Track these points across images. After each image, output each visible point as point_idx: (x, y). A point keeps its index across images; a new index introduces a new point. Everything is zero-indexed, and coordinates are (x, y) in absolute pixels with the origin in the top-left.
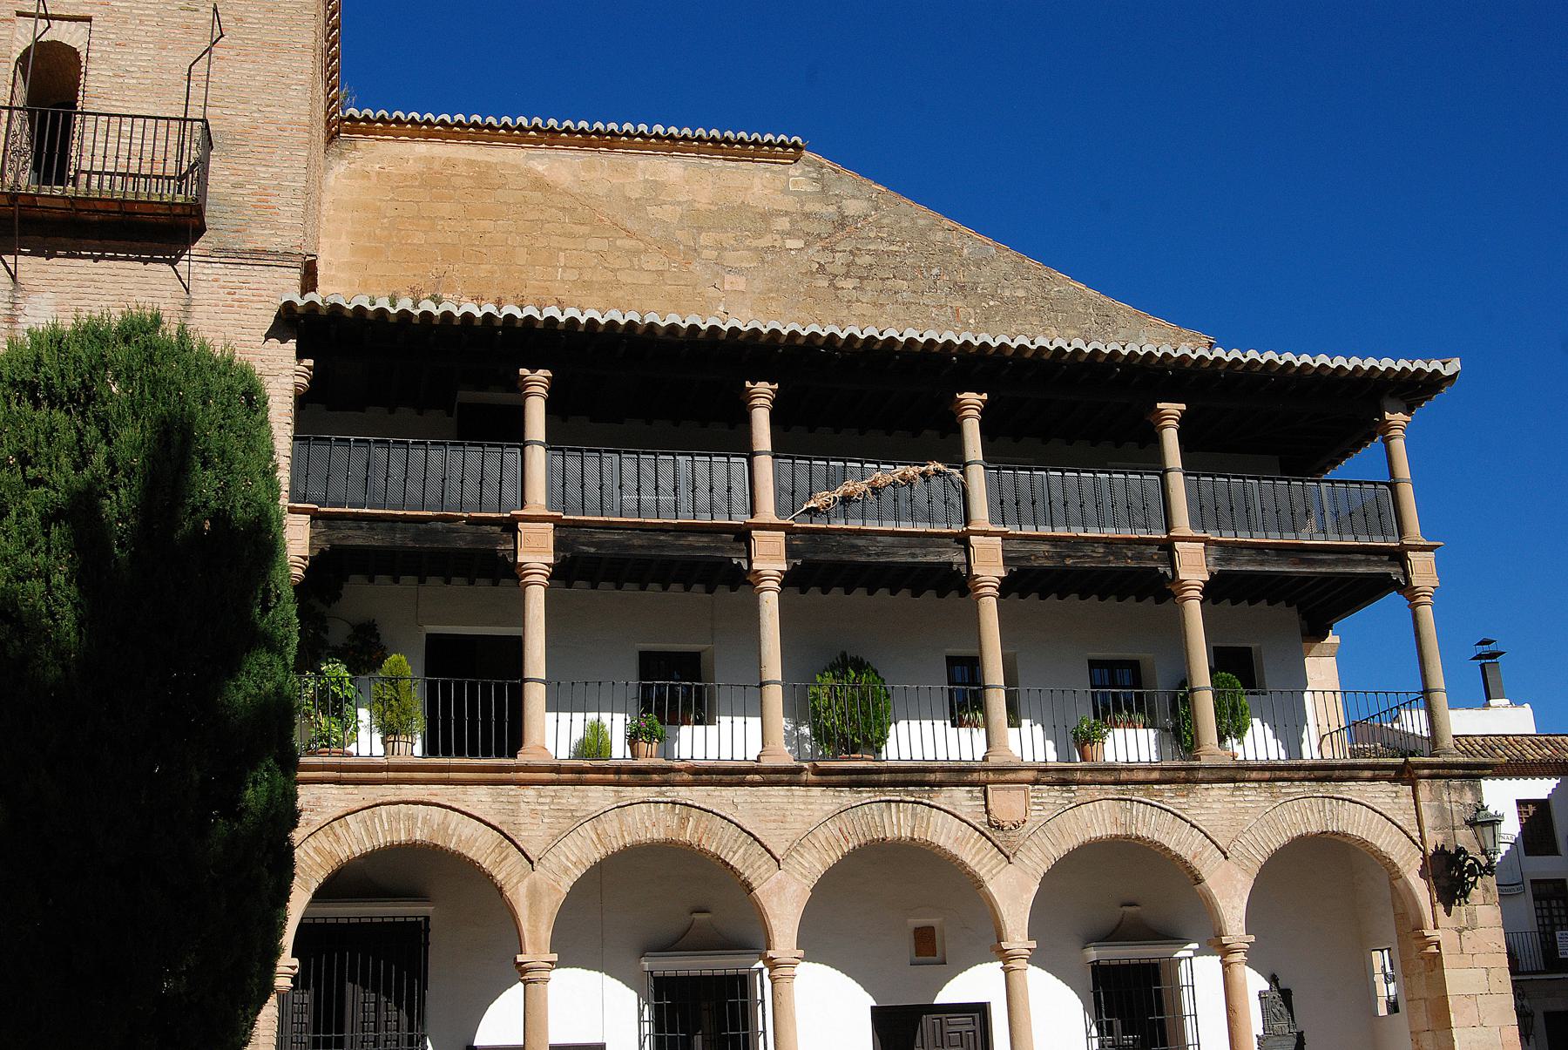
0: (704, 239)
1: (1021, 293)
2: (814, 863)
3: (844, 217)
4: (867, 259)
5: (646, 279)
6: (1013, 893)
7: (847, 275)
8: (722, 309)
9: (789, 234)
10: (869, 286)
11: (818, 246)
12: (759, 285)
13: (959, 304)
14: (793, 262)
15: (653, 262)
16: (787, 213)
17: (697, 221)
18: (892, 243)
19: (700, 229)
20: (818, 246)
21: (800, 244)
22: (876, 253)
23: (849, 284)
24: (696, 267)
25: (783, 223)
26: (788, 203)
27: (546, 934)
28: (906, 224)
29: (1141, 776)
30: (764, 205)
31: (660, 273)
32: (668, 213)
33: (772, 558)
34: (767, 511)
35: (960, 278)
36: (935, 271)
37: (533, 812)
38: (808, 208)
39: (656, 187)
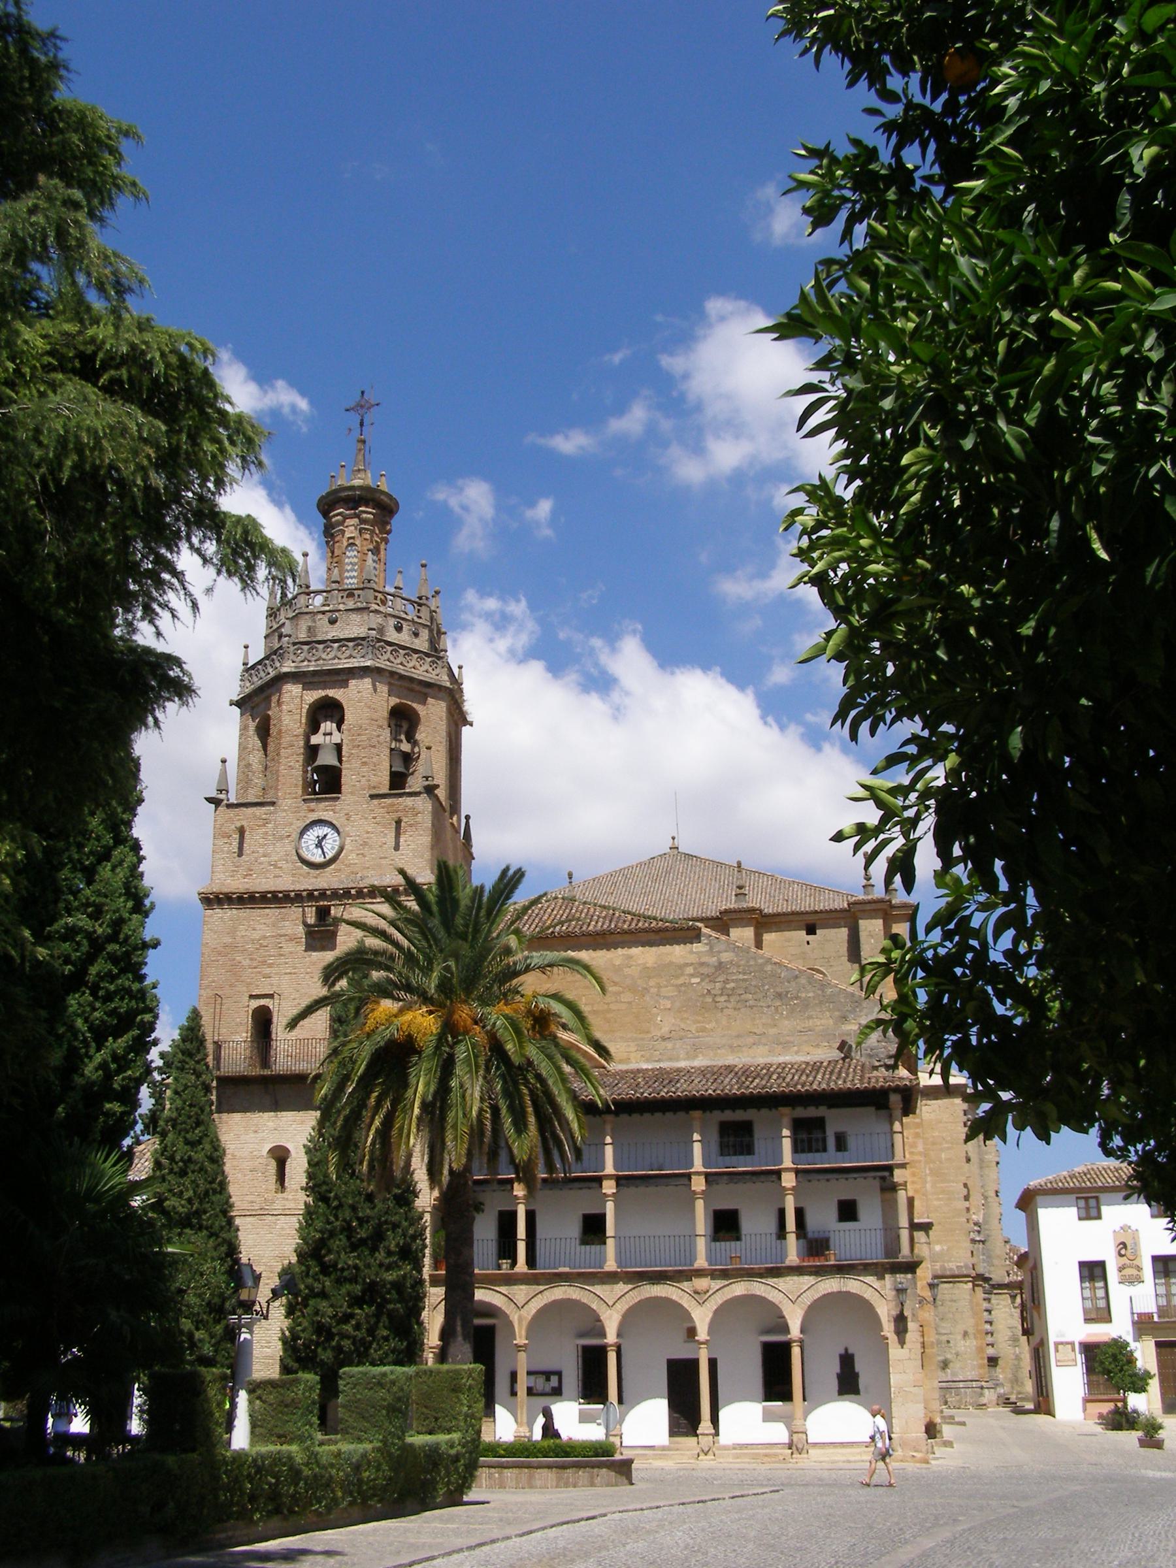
0: (652, 983)
1: (811, 995)
2: (622, 1307)
3: (720, 963)
4: (732, 985)
5: (624, 1006)
6: (702, 1318)
7: (721, 995)
9: (692, 976)
12: (678, 1004)
15: (627, 997)
17: (648, 972)
18: (744, 974)
19: (649, 978)
21: (698, 980)
23: (722, 999)
24: (647, 998)
25: (690, 970)
26: (693, 959)
27: (524, 1333)
28: (752, 963)
30: (682, 961)
31: (630, 1003)
34: (609, 1169)
37: (520, 1292)
38: (703, 960)
39: (630, 957)
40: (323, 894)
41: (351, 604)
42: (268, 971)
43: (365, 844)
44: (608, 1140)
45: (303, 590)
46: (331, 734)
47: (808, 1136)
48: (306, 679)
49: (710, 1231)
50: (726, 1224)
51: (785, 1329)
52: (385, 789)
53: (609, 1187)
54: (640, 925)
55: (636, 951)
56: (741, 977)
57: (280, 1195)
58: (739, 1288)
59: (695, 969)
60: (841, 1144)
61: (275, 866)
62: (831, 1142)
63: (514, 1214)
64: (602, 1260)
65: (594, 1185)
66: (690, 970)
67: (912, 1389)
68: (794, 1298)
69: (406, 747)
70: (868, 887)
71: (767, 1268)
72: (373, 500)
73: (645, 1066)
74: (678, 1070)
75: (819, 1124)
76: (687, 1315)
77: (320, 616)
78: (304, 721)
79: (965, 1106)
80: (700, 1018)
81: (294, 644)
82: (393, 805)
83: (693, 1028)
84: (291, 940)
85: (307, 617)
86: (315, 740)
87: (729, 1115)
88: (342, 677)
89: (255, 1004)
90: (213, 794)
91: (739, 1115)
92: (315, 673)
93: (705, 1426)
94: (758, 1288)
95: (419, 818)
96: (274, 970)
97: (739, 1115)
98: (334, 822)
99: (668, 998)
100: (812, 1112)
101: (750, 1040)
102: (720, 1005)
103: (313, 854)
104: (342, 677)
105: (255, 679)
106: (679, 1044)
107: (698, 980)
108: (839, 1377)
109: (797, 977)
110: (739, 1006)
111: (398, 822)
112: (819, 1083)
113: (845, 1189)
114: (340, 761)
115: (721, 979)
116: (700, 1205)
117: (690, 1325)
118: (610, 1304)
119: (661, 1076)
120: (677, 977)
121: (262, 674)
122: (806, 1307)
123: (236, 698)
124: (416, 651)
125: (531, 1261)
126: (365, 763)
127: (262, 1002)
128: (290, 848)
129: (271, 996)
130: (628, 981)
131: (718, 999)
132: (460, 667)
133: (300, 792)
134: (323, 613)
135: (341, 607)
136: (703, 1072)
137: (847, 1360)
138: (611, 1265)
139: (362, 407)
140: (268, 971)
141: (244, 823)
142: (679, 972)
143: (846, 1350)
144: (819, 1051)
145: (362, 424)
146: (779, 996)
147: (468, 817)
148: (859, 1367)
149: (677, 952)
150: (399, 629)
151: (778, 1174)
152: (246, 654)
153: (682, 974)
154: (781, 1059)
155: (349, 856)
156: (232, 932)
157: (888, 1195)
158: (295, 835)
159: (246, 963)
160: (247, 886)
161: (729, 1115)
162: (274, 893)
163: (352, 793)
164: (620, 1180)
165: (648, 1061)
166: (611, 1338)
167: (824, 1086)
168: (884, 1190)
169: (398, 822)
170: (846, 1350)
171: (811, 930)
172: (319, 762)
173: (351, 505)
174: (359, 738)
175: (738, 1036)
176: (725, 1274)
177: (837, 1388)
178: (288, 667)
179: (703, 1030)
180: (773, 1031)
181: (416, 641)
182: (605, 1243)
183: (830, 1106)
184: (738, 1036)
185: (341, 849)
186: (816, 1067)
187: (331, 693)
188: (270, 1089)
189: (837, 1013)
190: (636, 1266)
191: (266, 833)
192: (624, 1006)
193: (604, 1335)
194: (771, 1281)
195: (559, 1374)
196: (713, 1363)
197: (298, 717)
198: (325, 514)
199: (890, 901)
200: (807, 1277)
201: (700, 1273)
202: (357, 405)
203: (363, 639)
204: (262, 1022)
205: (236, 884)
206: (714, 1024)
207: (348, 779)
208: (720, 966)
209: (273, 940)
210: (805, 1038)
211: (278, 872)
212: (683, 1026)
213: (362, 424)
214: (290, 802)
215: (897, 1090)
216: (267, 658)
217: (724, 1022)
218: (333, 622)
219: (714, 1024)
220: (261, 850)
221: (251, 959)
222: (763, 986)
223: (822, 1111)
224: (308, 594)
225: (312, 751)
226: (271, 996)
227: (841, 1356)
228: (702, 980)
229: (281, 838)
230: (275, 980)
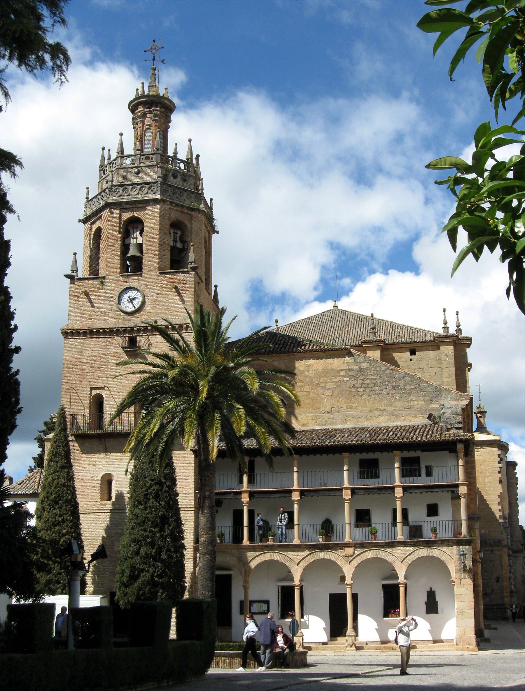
0: (321, 380)
1: (412, 387)
2: (303, 565)
3: (360, 369)
4: (367, 382)
5: (305, 394)
6: (348, 570)
7: (361, 387)
8: (325, 401)
9: (344, 376)
10: (367, 389)
11: (353, 379)
13: (393, 392)
14: (346, 385)
15: (307, 388)
16: (344, 370)
18: (374, 375)
19: (320, 377)
20: (353, 379)
21: (348, 379)
22: (369, 379)
23: (362, 390)
24: (319, 389)
25: (343, 373)
26: (345, 367)
28: (378, 369)
30: (338, 368)
31: (309, 392)
32: (311, 374)
33: (297, 497)
35: (394, 384)
36: (387, 383)
38: (350, 367)
39: (309, 366)
40: (132, 330)
41: (147, 163)
42: (101, 374)
43: (156, 301)
44: (295, 469)
47: (410, 468)
48: (123, 206)
49: (353, 522)
50: (362, 518)
51: (396, 577)
54: (314, 347)
55: (312, 362)
56: (372, 377)
58: (370, 554)
59: (346, 372)
60: (429, 472)
62: (423, 471)
63: (242, 511)
64: (292, 538)
65: (287, 495)
66: (343, 373)
67: (468, 611)
68: (401, 560)
69: (179, 245)
70: (446, 328)
71: (386, 543)
72: (161, 103)
73: (317, 428)
74: (336, 430)
75: (417, 461)
76: (340, 569)
77: (130, 170)
79: (499, 452)
80: (348, 401)
82: (171, 279)
83: (345, 406)
84: (114, 356)
85: (122, 171)
87: (365, 456)
88: (143, 204)
89: (94, 392)
90: (69, 273)
91: (371, 456)
92: (127, 203)
93: (350, 631)
94: (381, 554)
95: (188, 286)
96: (105, 373)
97: (371, 456)
98: (139, 288)
99: (329, 389)
100: (412, 454)
101: (377, 413)
102: (360, 393)
104: (143, 204)
105: (93, 207)
106: (336, 415)
107: (348, 379)
108: (426, 603)
109: (404, 377)
110: (371, 393)
111: (176, 288)
112: (416, 437)
113: (431, 498)
114: (142, 253)
115: (361, 378)
116: (347, 506)
117: (342, 575)
118: (297, 562)
119: (327, 433)
120: (336, 377)
121: (97, 204)
122: (408, 565)
123: (82, 218)
124: (185, 190)
125: (251, 538)
127: (98, 392)
129: (103, 388)
130: (307, 380)
131: (359, 390)
132: (211, 200)
133: (119, 271)
134: (132, 168)
135: (142, 165)
136: (351, 431)
137: (431, 594)
138: (296, 541)
140: (101, 374)
141: (87, 289)
142: (337, 374)
143: (431, 588)
144: (417, 419)
145: (154, 59)
146: (394, 388)
147: (216, 286)
149: (336, 363)
150: (175, 177)
151: (393, 488)
152: (88, 193)
153: (339, 376)
154: (395, 424)
155: (148, 307)
156: (81, 352)
157: (456, 502)
158: (116, 297)
160: (89, 325)
161: (365, 456)
162: (104, 330)
163: (149, 272)
164: (303, 493)
165: (319, 425)
166: (297, 582)
167: (419, 439)
168: (452, 498)
169: (176, 288)
170: (431, 588)
171: (413, 353)
173: (147, 106)
174: (153, 240)
175: (370, 411)
176: (362, 546)
179: (351, 407)
180: (390, 408)
181: (186, 184)
182: (294, 528)
183: (423, 451)
184: (370, 411)
186: (415, 428)
187: (136, 214)
188: (101, 439)
189: (427, 398)
190: (311, 541)
191: (99, 295)
192: (305, 394)
193: (293, 580)
194: (388, 550)
195: (267, 602)
196: (355, 597)
198: (133, 111)
199: (457, 336)
200: (409, 548)
201: (348, 545)
202: (151, 48)
204: (98, 403)
205: (83, 324)
206: (356, 404)
208: (360, 371)
209: (104, 356)
210: (409, 412)
211: (106, 317)
212: (339, 405)
213: (154, 59)
215: (461, 441)
216: (100, 194)
217: (362, 402)
218: (138, 173)
219: (356, 404)
222: (385, 382)
223: (418, 453)
224: (123, 157)
225: (125, 248)
226: (103, 388)
227: (428, 592)
228: (350, 379)
229: (108, 298)
230: (104, 379)
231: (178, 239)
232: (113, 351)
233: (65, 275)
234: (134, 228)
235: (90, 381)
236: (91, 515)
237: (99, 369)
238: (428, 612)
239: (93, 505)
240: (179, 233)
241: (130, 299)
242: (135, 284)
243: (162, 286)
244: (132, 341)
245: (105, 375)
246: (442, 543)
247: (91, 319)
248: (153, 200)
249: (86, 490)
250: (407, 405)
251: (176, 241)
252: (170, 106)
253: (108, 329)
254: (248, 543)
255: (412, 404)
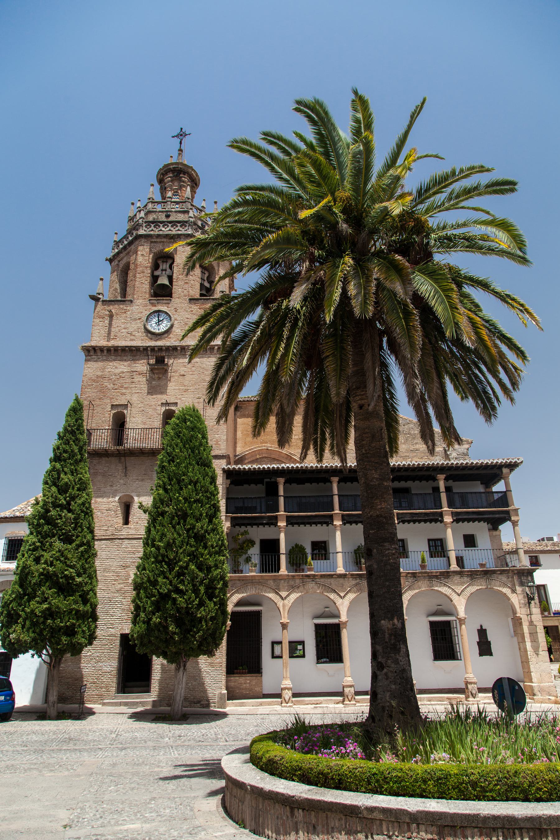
29: (434, 574)
40: (160, 349)
42: (124, 391)
45: (151, 200)
46: (166, 270)
52: (198, 296)
53: (338, 523)
57: (125, 526)
61: (131, 334)
64: (335, 567)
71: (440, 572)
78: (150, 261)
81: (146, 222)
84: (139, 374)
86: (157, 273)
103: (154, 329)
108: (478, 643)
126: (187, 283)
128: (141, 325)
133: (147, 296)
134: (162, 212)
137: (482, 633)
139: (181, 135)
140: (124, 391)
143: (481, 626)
148: (490, 637)
159: (111, 386)
170: (481, 626)
172: (159, 282)
177: (478, 652)
178: (141, 232)
185: (172, 326)
193: (338, 616)
195: (302, 643)
197: (147, 258)
203: (186, 222)
207: (177, 289)
209: (128, 374)
210: (415, 454)
211: (132, 337)
214: (141, 301)
220: (123, 326)
221: (114, 384)
225: (155, 278)
227: (478, 630)
229: (135, 320)
231: (205, 279)
232: (138, 370)
233: (90, 296)
234: (163, 262)
235: (111, 399)
236: (103, 542)
237: (122, 386)
238: (481, 655)
239: (107, 530)
240: (207, 275)
241: (159, 322)
242: (164, 308)
243: (192, 311)
244: (160, 361)
245: (129, 393)
246: (501, 574)
247: (116, 339)
248: (184, 235)
249: (99, 513)
250: (412, 448)
251: (204, 280)
252: (196, 179)
253: (134, 347)
254: (286, 573)
255: (417, 447)
